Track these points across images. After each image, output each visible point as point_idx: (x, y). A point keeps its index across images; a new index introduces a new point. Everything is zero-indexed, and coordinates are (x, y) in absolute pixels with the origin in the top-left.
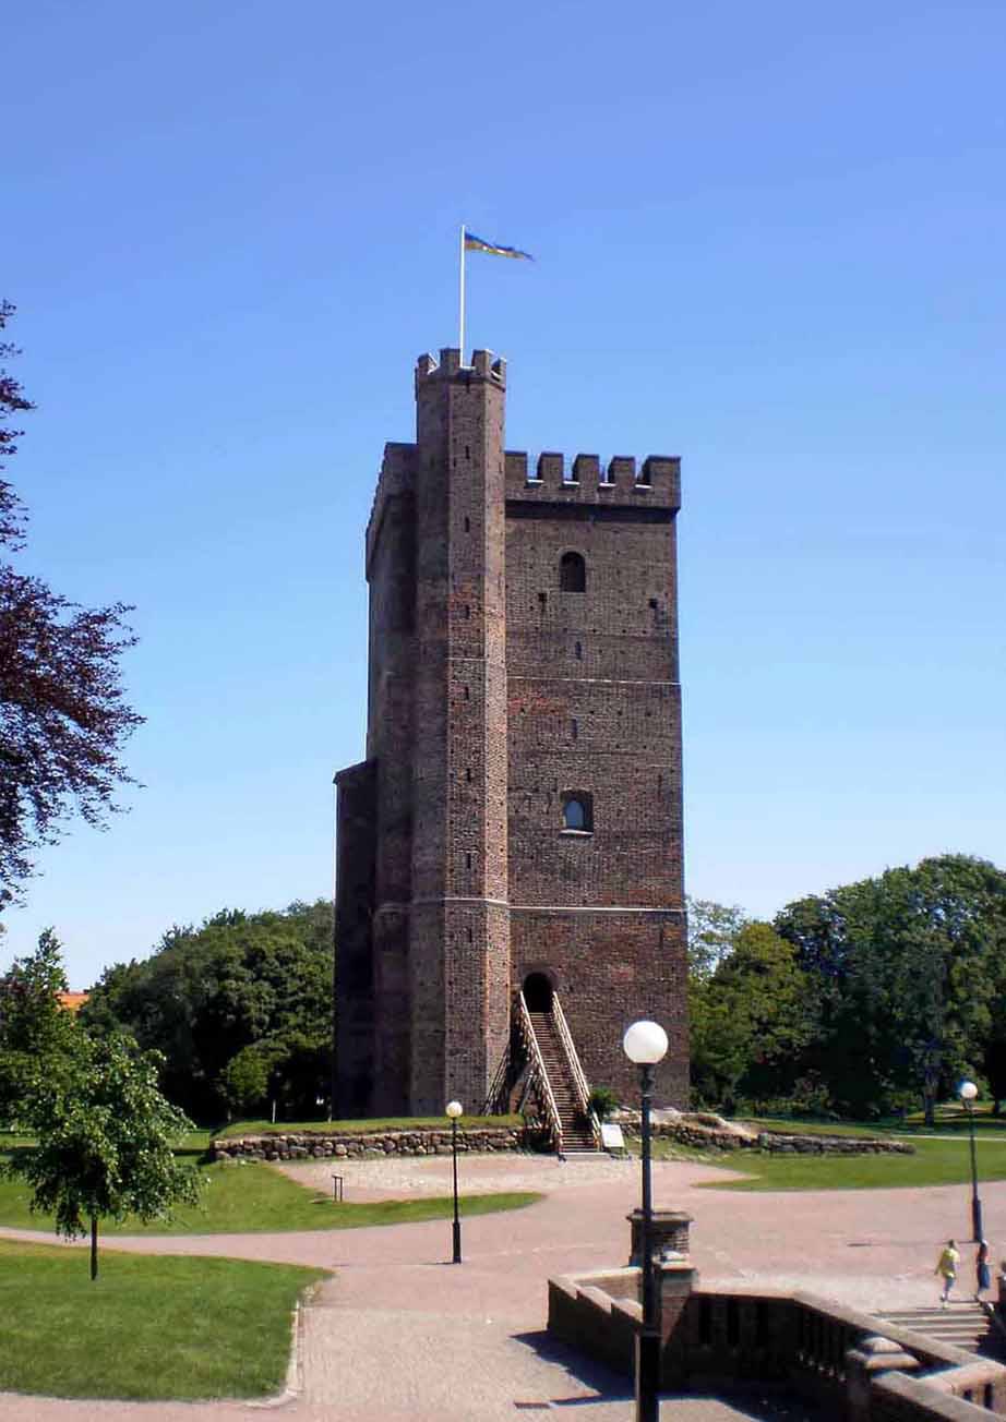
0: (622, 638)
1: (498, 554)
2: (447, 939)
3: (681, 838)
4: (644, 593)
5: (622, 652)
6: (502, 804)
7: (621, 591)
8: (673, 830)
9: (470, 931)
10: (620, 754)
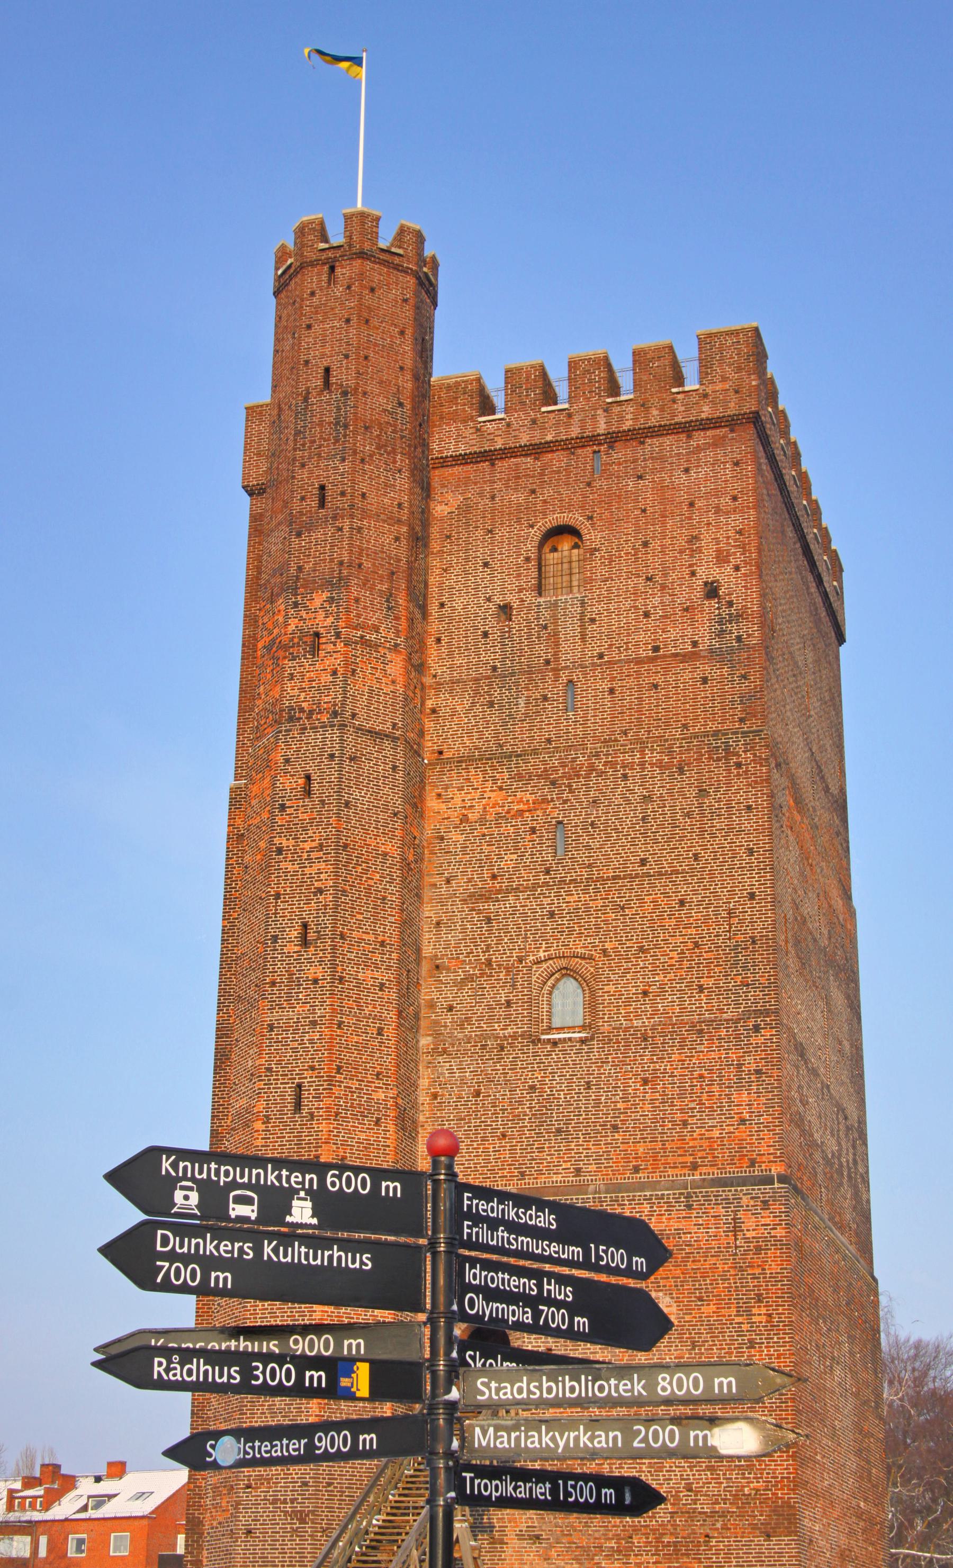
0: (652, 660)
1: (387, 540)
4: (693, 574)
5: (656, 686)
7: (649, 579)
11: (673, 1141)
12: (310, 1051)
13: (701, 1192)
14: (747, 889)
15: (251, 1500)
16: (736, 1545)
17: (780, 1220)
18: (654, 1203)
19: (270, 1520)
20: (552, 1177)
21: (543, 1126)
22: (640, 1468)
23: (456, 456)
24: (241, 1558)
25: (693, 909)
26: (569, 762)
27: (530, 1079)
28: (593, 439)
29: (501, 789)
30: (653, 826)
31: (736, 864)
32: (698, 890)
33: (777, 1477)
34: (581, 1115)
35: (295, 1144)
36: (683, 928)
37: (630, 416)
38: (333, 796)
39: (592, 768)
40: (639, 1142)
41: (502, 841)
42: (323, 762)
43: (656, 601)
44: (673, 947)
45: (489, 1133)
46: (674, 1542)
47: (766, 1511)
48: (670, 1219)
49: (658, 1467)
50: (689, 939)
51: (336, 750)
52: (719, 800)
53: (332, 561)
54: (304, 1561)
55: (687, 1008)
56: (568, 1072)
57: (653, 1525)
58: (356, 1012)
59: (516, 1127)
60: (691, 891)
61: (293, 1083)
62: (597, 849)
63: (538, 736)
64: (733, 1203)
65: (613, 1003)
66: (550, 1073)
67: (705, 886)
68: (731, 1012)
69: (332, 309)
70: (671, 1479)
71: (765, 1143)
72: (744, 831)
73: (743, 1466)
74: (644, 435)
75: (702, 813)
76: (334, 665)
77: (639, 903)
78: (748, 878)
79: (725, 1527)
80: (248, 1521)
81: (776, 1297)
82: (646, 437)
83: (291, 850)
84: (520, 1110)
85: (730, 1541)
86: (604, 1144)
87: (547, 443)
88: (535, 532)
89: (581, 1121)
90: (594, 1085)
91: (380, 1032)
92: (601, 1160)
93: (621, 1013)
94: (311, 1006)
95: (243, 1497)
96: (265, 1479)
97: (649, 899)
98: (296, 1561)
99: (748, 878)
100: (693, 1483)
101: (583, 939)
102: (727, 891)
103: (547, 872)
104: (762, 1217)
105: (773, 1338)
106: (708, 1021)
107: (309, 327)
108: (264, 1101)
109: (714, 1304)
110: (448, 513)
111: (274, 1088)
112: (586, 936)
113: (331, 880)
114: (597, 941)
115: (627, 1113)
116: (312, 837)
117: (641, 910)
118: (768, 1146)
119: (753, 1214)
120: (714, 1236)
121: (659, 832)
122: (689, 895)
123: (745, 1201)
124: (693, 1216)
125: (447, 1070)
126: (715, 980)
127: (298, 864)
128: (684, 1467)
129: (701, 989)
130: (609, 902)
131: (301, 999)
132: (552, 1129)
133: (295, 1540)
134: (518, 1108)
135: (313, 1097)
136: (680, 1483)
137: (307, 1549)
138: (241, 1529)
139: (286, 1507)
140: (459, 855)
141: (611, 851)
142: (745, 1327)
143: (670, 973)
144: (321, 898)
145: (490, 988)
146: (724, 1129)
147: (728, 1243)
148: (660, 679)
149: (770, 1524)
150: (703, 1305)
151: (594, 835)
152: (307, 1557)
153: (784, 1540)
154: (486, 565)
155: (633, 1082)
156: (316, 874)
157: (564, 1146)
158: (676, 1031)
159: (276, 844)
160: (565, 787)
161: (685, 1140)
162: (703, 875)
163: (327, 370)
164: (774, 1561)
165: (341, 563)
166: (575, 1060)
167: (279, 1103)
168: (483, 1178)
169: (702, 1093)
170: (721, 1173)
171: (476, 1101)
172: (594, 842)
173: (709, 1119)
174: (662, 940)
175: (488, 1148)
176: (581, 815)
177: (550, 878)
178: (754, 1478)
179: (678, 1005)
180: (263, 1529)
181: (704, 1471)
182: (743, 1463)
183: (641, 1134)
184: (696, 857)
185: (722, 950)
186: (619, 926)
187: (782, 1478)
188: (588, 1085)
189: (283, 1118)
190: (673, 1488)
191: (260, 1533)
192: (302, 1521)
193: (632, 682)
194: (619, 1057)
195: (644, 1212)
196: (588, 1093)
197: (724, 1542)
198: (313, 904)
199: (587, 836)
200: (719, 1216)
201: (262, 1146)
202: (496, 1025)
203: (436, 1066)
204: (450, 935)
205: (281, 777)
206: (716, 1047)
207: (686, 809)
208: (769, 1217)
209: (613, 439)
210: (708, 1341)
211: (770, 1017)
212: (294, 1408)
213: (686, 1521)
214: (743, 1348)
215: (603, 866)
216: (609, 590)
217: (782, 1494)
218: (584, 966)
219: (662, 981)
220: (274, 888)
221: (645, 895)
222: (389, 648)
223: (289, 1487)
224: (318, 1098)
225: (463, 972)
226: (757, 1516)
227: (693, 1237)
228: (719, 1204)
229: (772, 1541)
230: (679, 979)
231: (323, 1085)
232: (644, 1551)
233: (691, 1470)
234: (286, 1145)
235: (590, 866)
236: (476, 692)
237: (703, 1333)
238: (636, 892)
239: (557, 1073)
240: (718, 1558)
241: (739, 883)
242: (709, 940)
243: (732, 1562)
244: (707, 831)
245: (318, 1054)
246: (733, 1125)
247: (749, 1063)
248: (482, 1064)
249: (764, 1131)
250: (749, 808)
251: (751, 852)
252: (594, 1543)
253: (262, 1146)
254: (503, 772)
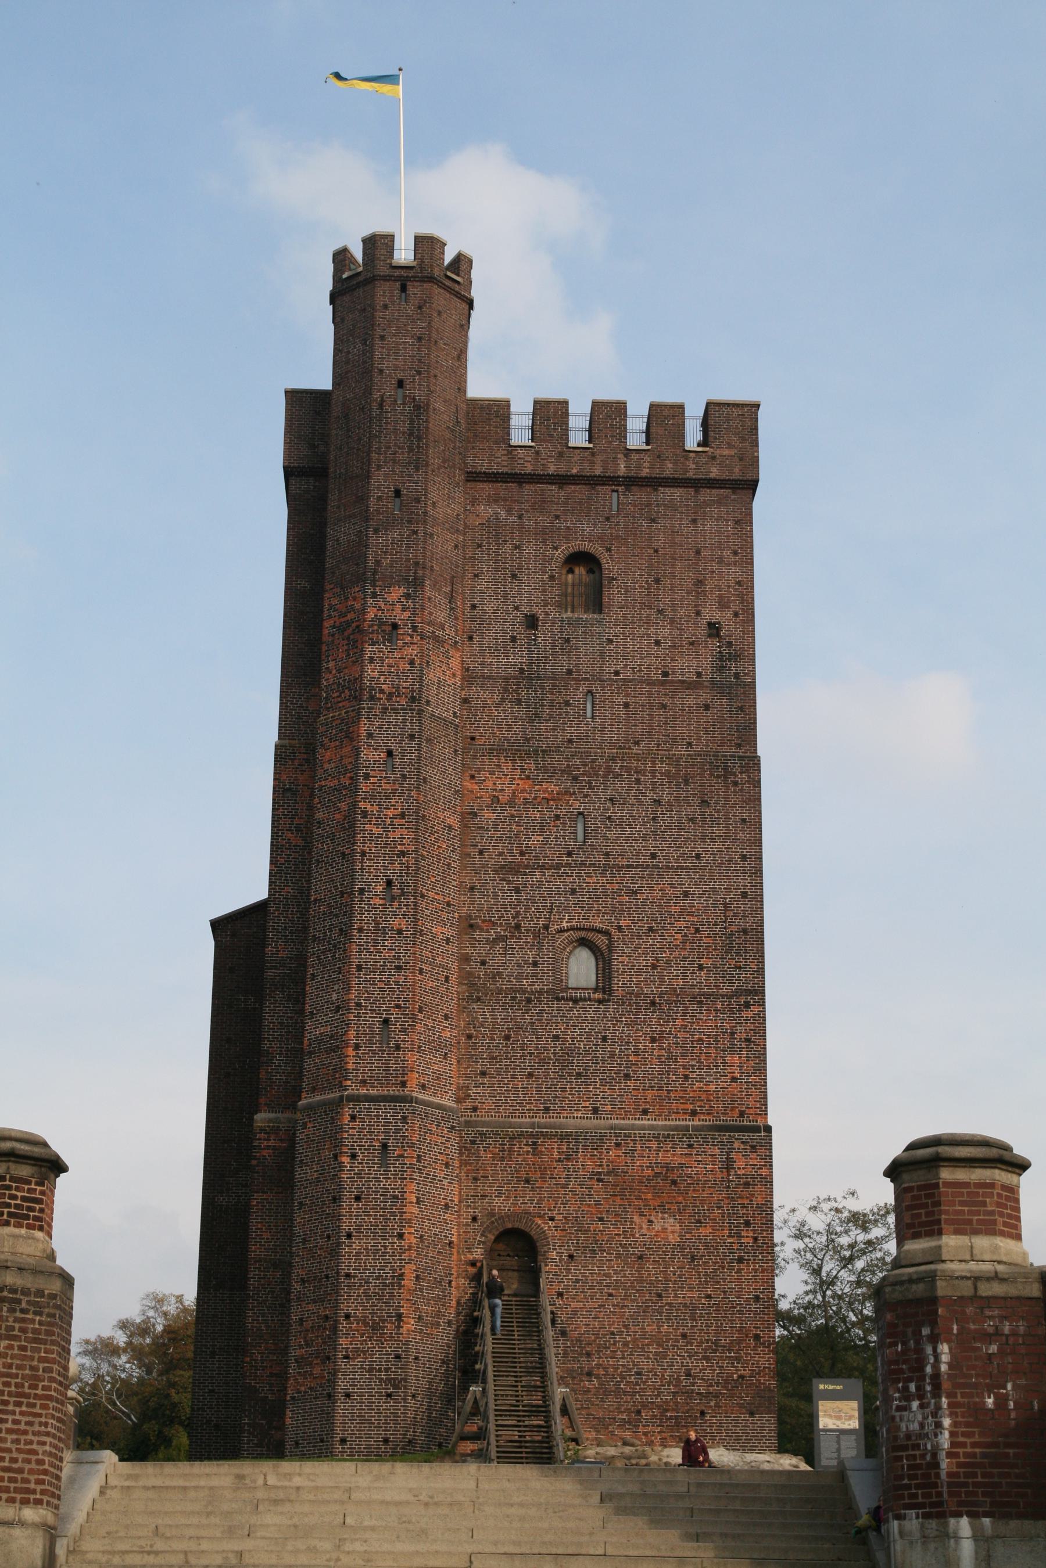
0: (663, 683)
1: (450, 546)
2: (346, 1160)
3: (763, 1004)
4: (698, 613)
5: (664, 706)
6: (448, 941)
7: (660, 612)
8: (748, 992)
9: (385, 1146)
11: (676, 1091)
12: (396, 991)
13: (700, 1135)
14: (740, 889)
15: (349, 1369)
16: (726, 1420)
17: (765, 1162)
18: (661, 1141)
19: (366, 1385)
20: (573, 1113)
21: (565, 1069)
22: (648, 1355)
23: (489, 473)
24: (340, 1416)
25: (695, 900)
26: (589, 762)
27: (554, 1029)
29: (528, 778)
30: (662, 826)
31: (732, 867)
32: (700, 885)
33: (761, 1367)
34: (599, 1063)
35: (383, 1070)
36: (687, 915)
37: (646, 465)
38: (414, 772)
39: (609, 770)
40: (648, 1090)
41: (530, 823)
42: (404, 741)
44: (678, 930)
45: (518, 1072)
46: (675, 1416)
47: (751, 1394)
48: (674, 1155)
49: (663, 1355)
50: (691, 924)
51: (416, 732)
52: (718, 811)
53: (408, 560)
54: (397, 1420)
55: (689, 982)
56: (588, 1026)
57: (658, 1402)
58: (431, 961)
59: (541, 1069)
60: (693, 885)
61: (380, 1018)
62: (613, 840)
63: (561, 736)
64: (727, 1145)
65: (626, 972)
66: (572, 1026)
67: (706, 882)
68: (726, 989)
69: (405, 325)
70: (674, 1366)
71: (753, 1098)
72: (739, 839)
73: (732, 1357)
74: (658, 484)
75: (704, 820)
76: (411, 655)
77: (650, 890)
78: (742, 879)
79: (717, 1405)
80: (347, 1386)
81: (761, 1224)
82: (659, 486)
83: (375, 815)
84: (545, 1055)
85: (721, 1417)
86: (618, 1089)
87: (572, 476)
88: (559, 554)
89: (598, 1068)
90: (609, 1039)
91: (447, 979)
92: (615, 1102)
93: (633, 981)
94: (396, 953)
95: (341, 1365)
96: (362, 1351)
97: (657, 887)
98: (390, 1420)
99: (742, 879)
100: (692, 1369)
101: (601, 915)
102: (724, 888)
103: (569, 854)
104: (750, 1159)
105: (758, 1256)
106: (707, 995)
107: (382, 338)
108: (354, 1031)
109: (710, 1226)
110: (479, 524)
111: (363, 1021)
112: (603, 913)
113: (413, 845)
114: (613, 918)
115: (638, 1065)
116: (395, 806)
117: (651, 896)
118: (755, 1101)
119: (743, 1155)
120: (711, 1171)
121: (667, 832)
122: (692, 888)
123: (736, 1145)
124: (694, 1153)
125: (480, 1015)
126: (713, 961)
127: (382, 828)
128: (684, 1356)
129: (701, 968)
130: (623, 886)
131: (387, 946)
132: (573, 1073)
133: (390, 1403)
134: (544, 1053)
135: (399, 1031)
136: (681, 1369)
137: (400, 1410)
138: (340, 1393)
139: (381, 1375)
140: (491, 831)
141: (626, 843)
143: (675, 951)
144: (404, 860)
145: (519, 948)
146: (719, 1085)
147: (722, 1178)
148: (669, 700)
149: (754, 1404)
150: (701, 1226)
151: (611, 828)
152: (400, 1417)
153: (765, 1417)
154: (514, 576)
155: (643, 1040)
156: (398, 838)
157: (583, 1088)
158: (680, 1001)
159: (361, 808)
160: (586, 783)
161: (686, 1091)
162: (704, 872)
163: (401, 384)
164: (757, 1433)
165: (417, 564)
166: (594, 1017)
167: (368, 1034)
168: (513, 1110)
169: (701, 1053)
170: (716, 1121)
171: (507, 1044)
172: (611, 834)
173: (706, 1075)
174: (668, 924)
175: (518, 1085)
176: (600, 810)
177: (572, 860)
178: (742, 1367)
179: (681, 979)
180: (360, 1392)
181: (700, 1359)
182: (732, 1355)
183: (649, 1083)
184: (698, 856)
185: (719, 937)
186: (632, 908)
187: (764, 1367)
188: (604, 1039)
189: (373, 1047)
190: (675, 1372)
191: (358, 1396)
192: (395, 1387)
193: (644, 700)
194: (631, 1018)
195: (653, 1147)
196: (605, 1045)
197: (716, 1417)
198: (396, 865)
199: (604, 828)
200: (716, 1155)
201: (353, 1069)
202: (525, 981)
203: (471, 1011)
204: (483, 900)
205: (364, 748)
206: (713, 1017)
207: (690, 815)
208: (757, 1159)
209: (632, 482)
210: (705, 1256)
211: (758, 996)
212: (387, 1293)
213: (685, 1399)
214: (733, 1263)
215: (618, 855)
216: (625, 616)
217: (764, 1380)
218: (600, 938)
219: (669, 957)
220: (360, 846)
221: (655, 884)
222: (451, 645)
223: (383, 1358)
224: (404, 1031)
225: (494, 932)
226: (743, 1397)
227: (693, 1171)
228: (715, 1145)
229: (756, 1417)
230: (683, 958)
231: (408, 1022)
232: (650, 1422)
233: (690, 1359)
234: (375, 1070)
235: (607, 854)
236: (506, 690)
237: (701, 1249)
238: (646, 880)
239: (578, 1026)
240: (712, 1430)
241: (734, 882)
242: (709, 928)
243: (723, 1433)
244: (708, 836)
245: (403, 995)
246: (727, 1082)
247: (741, 1033)
248: (512, 1013)
249: (752, 1089)
250: (744, 821)
251: (744, 858)
252: (609, 1415)
253: (353, 1069)
254: (531, 764)
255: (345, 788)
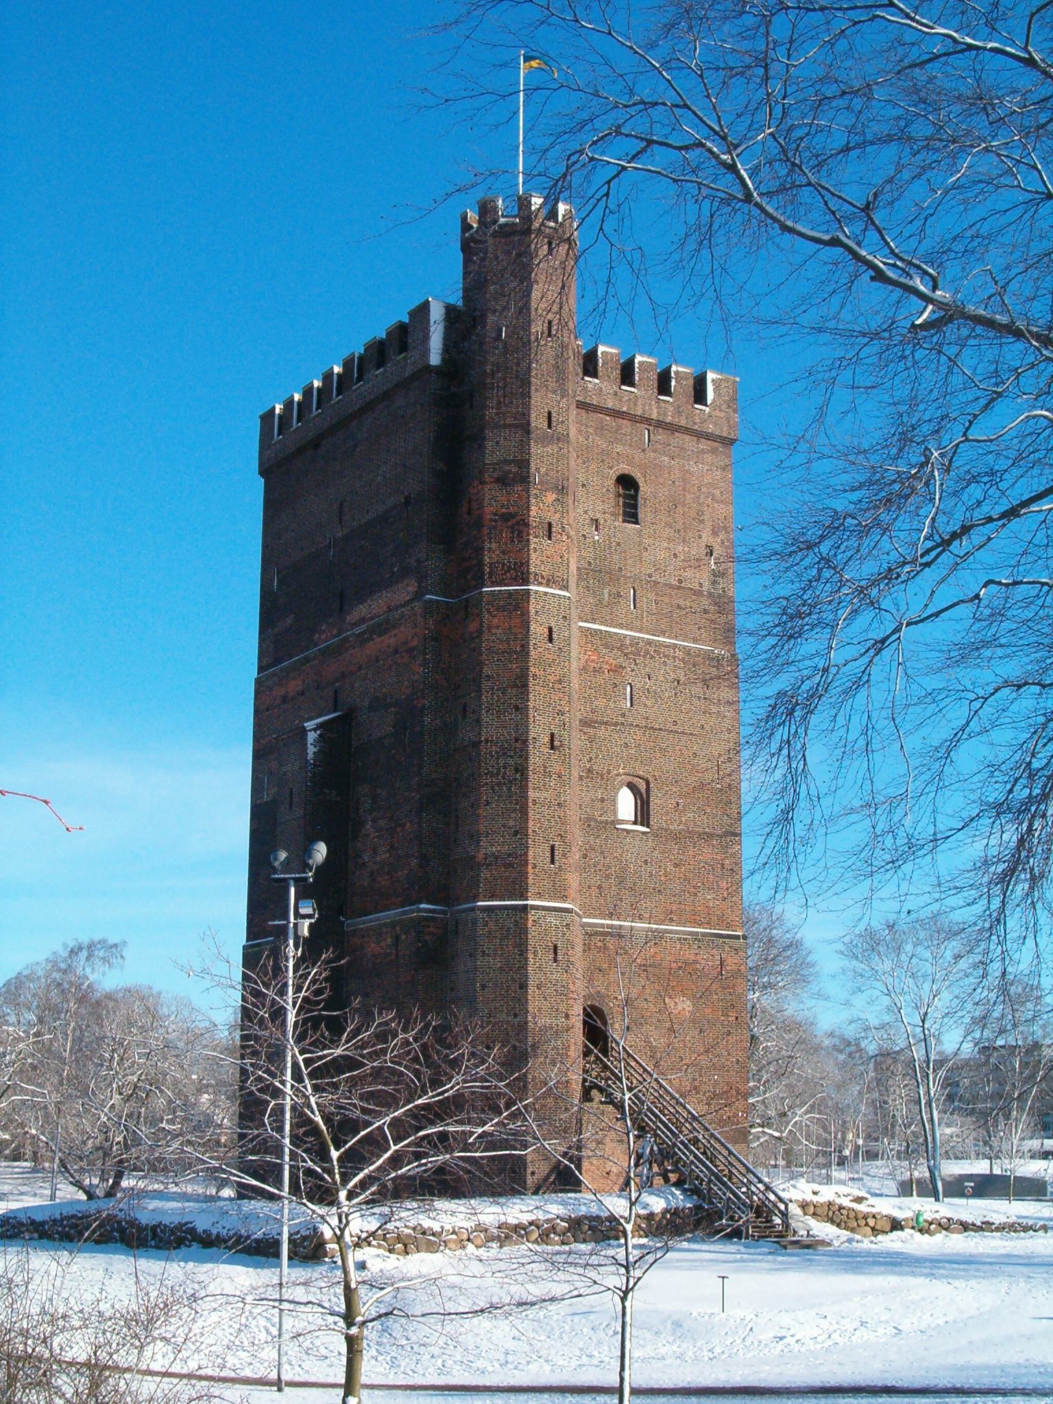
0: (679, 588)
5: (679, 607)
9: (555, 947)
10: (677, 732)
28: (646, 420)
39: (647, 653)
43: (680, 548)
103: (623, 715)
123: (727, 948)
142: (726, 1023)
154: (584, 485)
209: (660, 424)
235: (647, 718)
255: (515, 652)
